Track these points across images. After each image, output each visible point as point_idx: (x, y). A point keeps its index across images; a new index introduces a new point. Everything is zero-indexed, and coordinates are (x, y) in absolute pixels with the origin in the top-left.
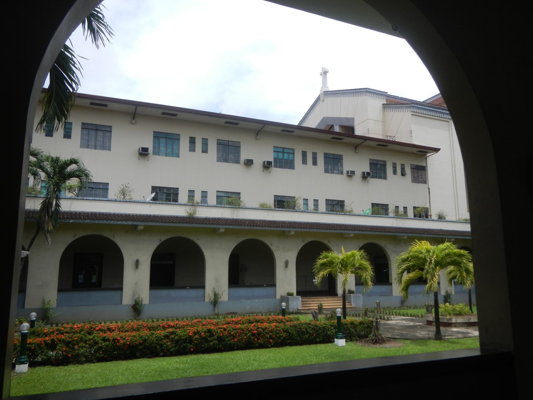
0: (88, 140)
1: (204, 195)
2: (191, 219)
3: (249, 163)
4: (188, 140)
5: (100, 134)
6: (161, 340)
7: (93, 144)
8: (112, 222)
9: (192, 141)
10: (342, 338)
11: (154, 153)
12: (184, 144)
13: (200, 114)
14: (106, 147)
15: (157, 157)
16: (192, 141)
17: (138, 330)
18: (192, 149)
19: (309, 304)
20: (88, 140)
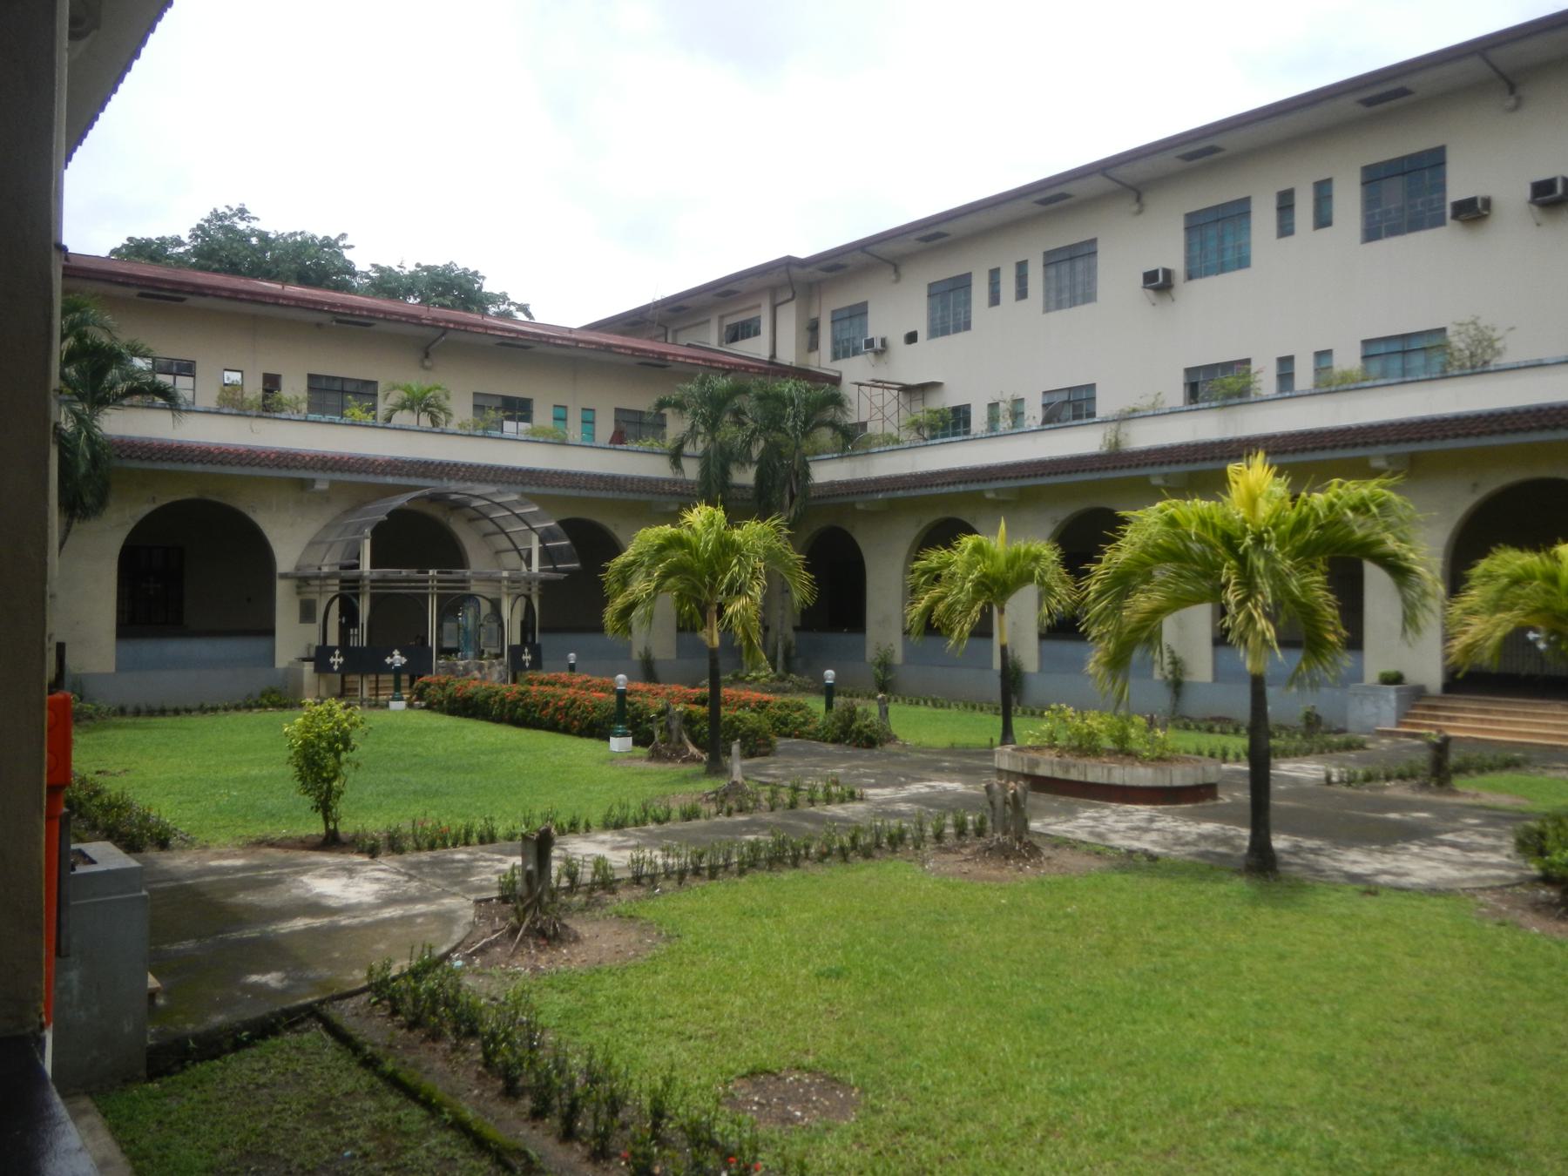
0: (1059, 291)
1: (1286, 366)
2: (1115, 458)
3: (1473, 212)
4: (1272, 203)
5: (1080, 265)
6: (490, 697)
7: (1066, 295)
8: (935, 490)
9: (1286, 204)
10: (615, 735)
11: (1190, 276)
12: (1264, 217)
13: (1263, 119)
14: (1089, 296)
15: (1199, 284)
16: (1286, 204)
17: (553, 685)
18: (1285, 228)
19: (1449, 719)
20: (1059, 291)
